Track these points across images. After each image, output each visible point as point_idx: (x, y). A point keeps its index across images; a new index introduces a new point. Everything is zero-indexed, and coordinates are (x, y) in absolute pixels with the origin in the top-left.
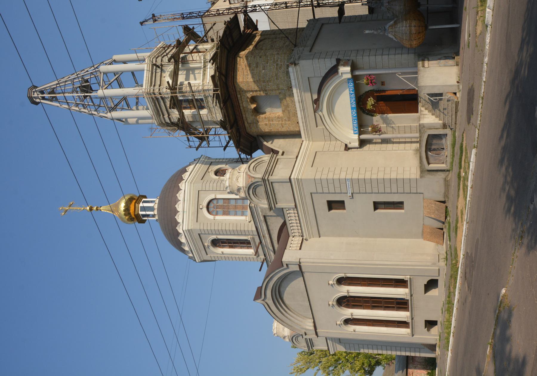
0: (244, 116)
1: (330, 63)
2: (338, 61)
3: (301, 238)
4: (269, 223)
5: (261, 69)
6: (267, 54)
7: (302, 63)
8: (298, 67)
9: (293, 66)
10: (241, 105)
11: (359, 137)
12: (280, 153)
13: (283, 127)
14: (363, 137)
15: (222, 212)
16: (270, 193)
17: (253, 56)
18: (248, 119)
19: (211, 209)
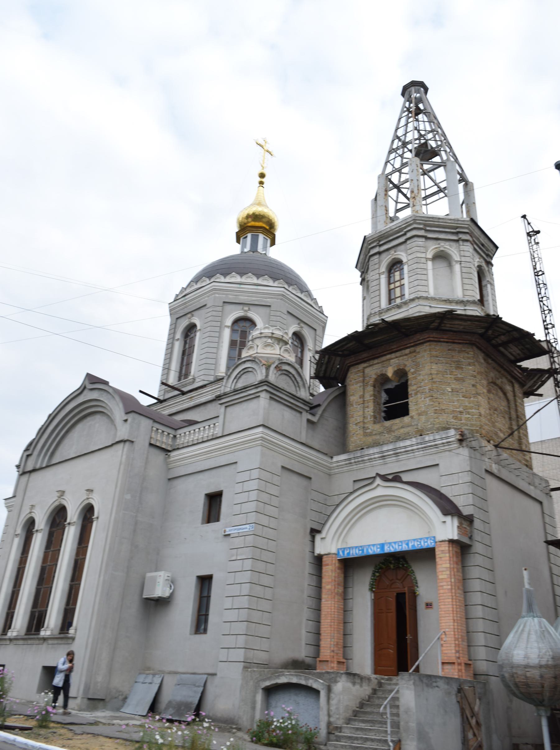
0: (376, 361)
1: (464, 503)
2: (469, 520)
3: (169, 449)
5: (453, 386)
6: (480, 398)
9: (458, 437)
10: (393, 355)
13: (356, 424)
17: (475, 374)
18: (371, 368)
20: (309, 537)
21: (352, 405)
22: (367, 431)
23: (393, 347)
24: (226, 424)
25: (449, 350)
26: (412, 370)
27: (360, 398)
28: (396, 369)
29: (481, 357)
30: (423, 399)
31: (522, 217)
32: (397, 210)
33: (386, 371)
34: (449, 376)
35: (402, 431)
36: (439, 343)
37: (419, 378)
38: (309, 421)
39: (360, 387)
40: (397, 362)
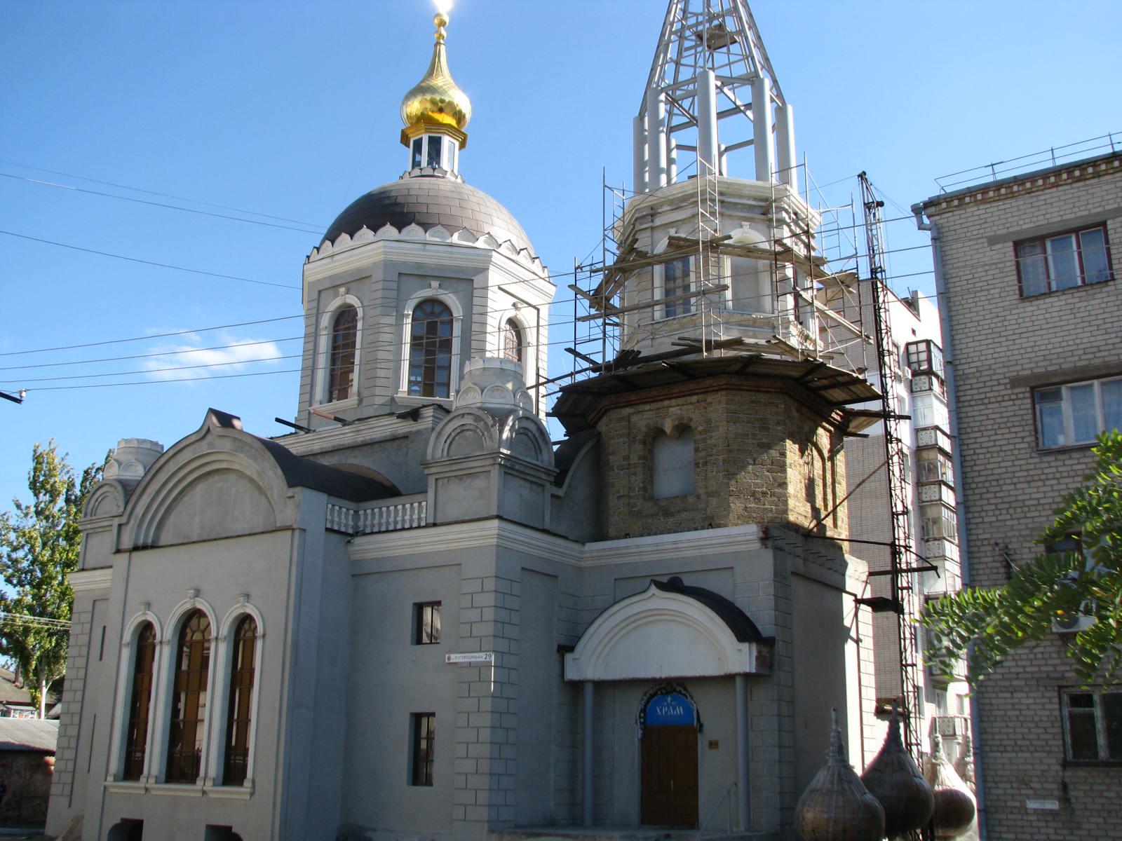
0: (647, 407)
1: (764, 618)
3: (350, 531)
4: (389, 445)
7: (767, 558)
8: (757, 545)
10: (673, 402)
11: (589, 681)
12: (555, 491)
13: (619, 498)
14: (589, 691)
15: (419, 334)
16: (463, 466)
19: (428, 308)
20: (555, 657)
21: (612, 469)
22: (634, 509)
23: (674, 391)
24: (439, 505)
25: (752, 402)
26: (700, 428)
27: (624, 460)
28: (677, 423)
29: (793, 409)
30: (714, 473)
31: (859, 176)
32: (671, 128)
33: (662, 425)
34: (750, 441)
35: (684, 515)
36: (739, 392)
37: (709, 442)
38: (553, 496)
39: (624, 443)
40: (679, 412)
